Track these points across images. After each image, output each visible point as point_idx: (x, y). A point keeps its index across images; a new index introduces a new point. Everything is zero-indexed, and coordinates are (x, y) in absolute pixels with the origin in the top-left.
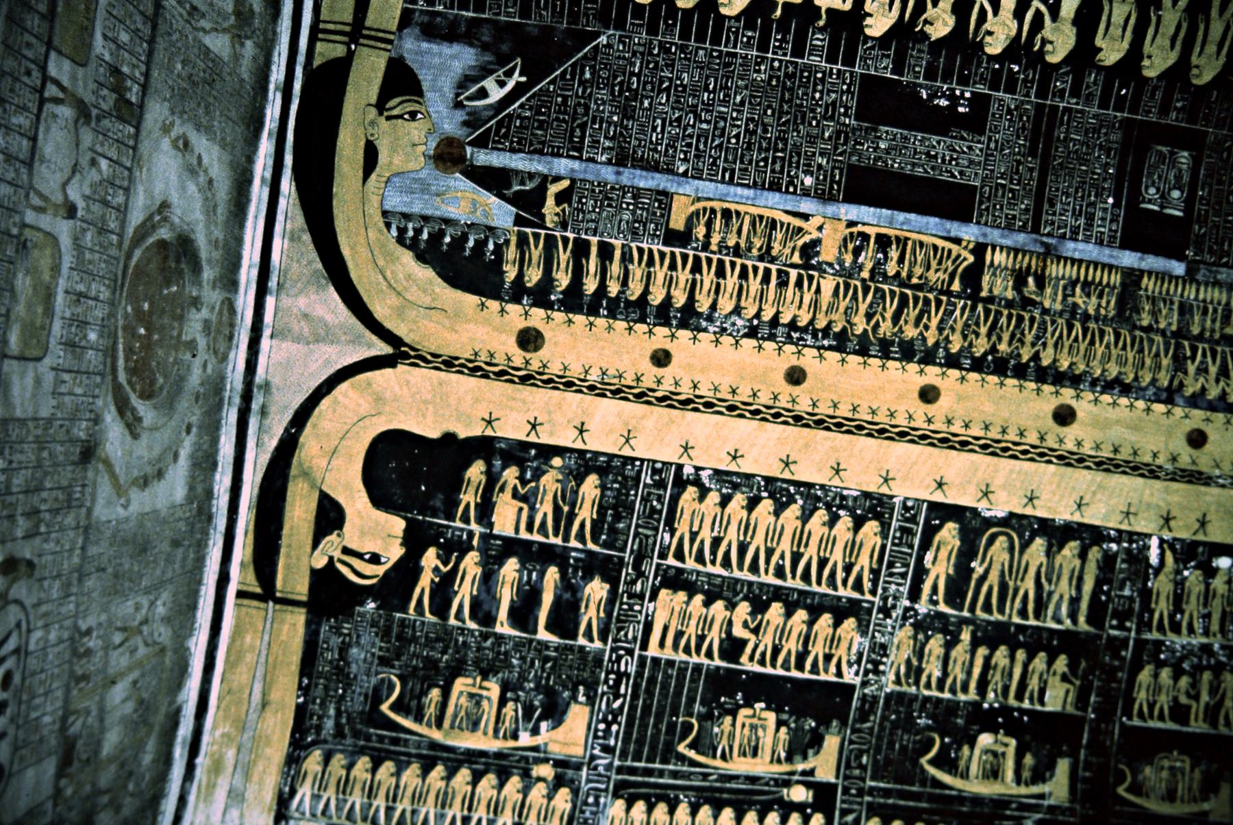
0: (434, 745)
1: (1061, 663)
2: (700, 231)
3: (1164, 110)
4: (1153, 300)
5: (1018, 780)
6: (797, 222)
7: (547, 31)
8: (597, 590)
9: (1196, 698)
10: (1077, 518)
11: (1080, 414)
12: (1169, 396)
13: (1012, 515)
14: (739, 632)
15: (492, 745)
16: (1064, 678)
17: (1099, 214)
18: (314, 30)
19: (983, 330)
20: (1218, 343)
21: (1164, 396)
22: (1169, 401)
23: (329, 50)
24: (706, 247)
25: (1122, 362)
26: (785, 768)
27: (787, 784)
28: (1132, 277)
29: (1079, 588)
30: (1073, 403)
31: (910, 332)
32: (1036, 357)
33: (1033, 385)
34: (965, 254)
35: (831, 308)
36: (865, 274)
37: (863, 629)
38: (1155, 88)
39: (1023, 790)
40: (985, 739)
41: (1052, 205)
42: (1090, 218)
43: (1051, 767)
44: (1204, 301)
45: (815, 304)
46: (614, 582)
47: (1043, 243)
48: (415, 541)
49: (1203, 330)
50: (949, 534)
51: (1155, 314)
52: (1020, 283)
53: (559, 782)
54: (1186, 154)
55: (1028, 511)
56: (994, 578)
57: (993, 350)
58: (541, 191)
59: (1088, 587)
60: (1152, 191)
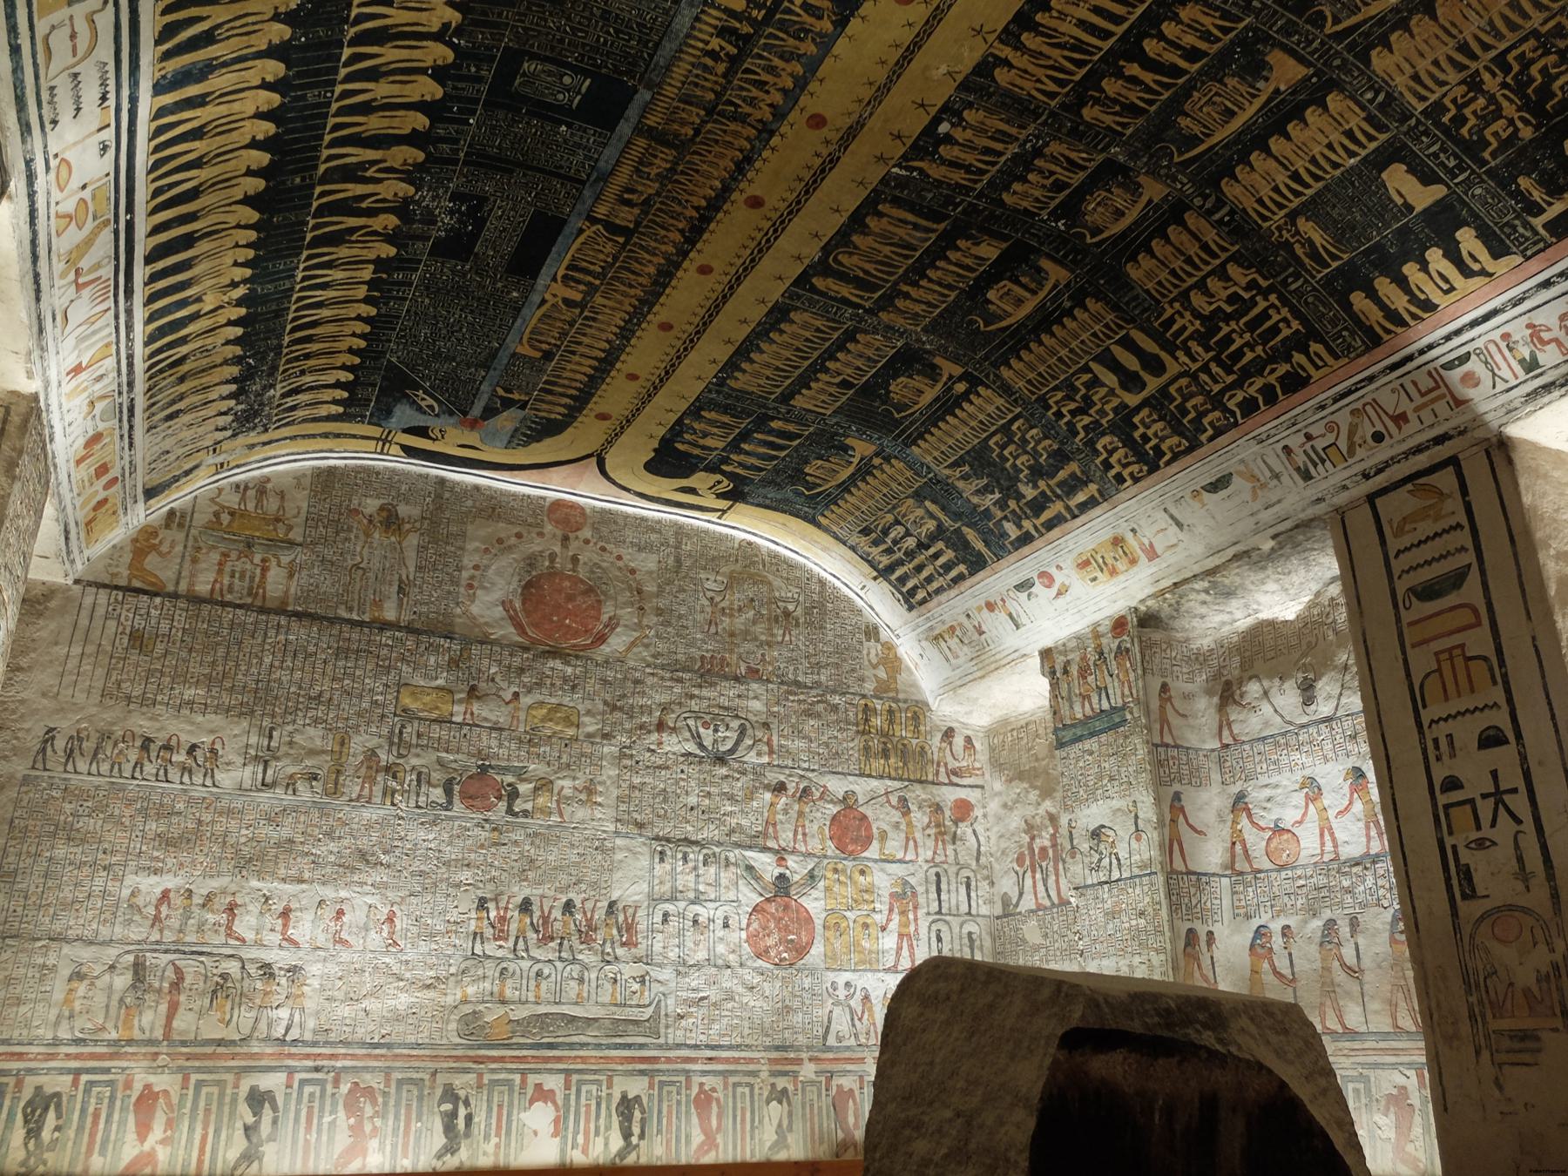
0: (839, 486)
1: (961, 243)
2: (545, 346)
3: (479, 79)
4: (669, 121)
5: (1034, 292)
6: (547, 306)
7: (384, 378)
8: (775, 424)
9: (1052, 173)
10: (846, 215)
11: (758, 193)
12: (766, 131)
13: (823, 248)
14: (837, 380)
15: (851, 470)
16: (978, 244)
17: (577, 139)
18: (382, 453)
19: (663, 233)
20: (730, 82)
21: (765, 135)
22: (772, 133)
23: (395, 449)
24: (559, 347)
25: (722, 156)
26: (940, 385)
27: (950, 389)
28: (639, 130)
29: (906, 222)
30: (745, 196)
31: (652, 270)
32: (697, 209)
33: (720, 215)
34: (594, 228)
35: (621, 303)
36: (597, 282)
37: (866, 332)
38: (455, 88)
39: (1042, 295)
40: (991, 295)
41: (561, 167)
42: (579, 146)
43: (1039, 270)
44: (683, 83)
45: (613, 309)
46: (773, 419)
47: (595, 181)
48: (712, 469)
49: (712, 90)
50: (818, 282)
51: (683, 123)
52: (628, 203)
53: (887, 459)
54: (526, 65)
55: (825, 240)
56: (867, 266)
57: (682, 231)
58: (501, 398)
59: (910, 217)
60: (560, 97)
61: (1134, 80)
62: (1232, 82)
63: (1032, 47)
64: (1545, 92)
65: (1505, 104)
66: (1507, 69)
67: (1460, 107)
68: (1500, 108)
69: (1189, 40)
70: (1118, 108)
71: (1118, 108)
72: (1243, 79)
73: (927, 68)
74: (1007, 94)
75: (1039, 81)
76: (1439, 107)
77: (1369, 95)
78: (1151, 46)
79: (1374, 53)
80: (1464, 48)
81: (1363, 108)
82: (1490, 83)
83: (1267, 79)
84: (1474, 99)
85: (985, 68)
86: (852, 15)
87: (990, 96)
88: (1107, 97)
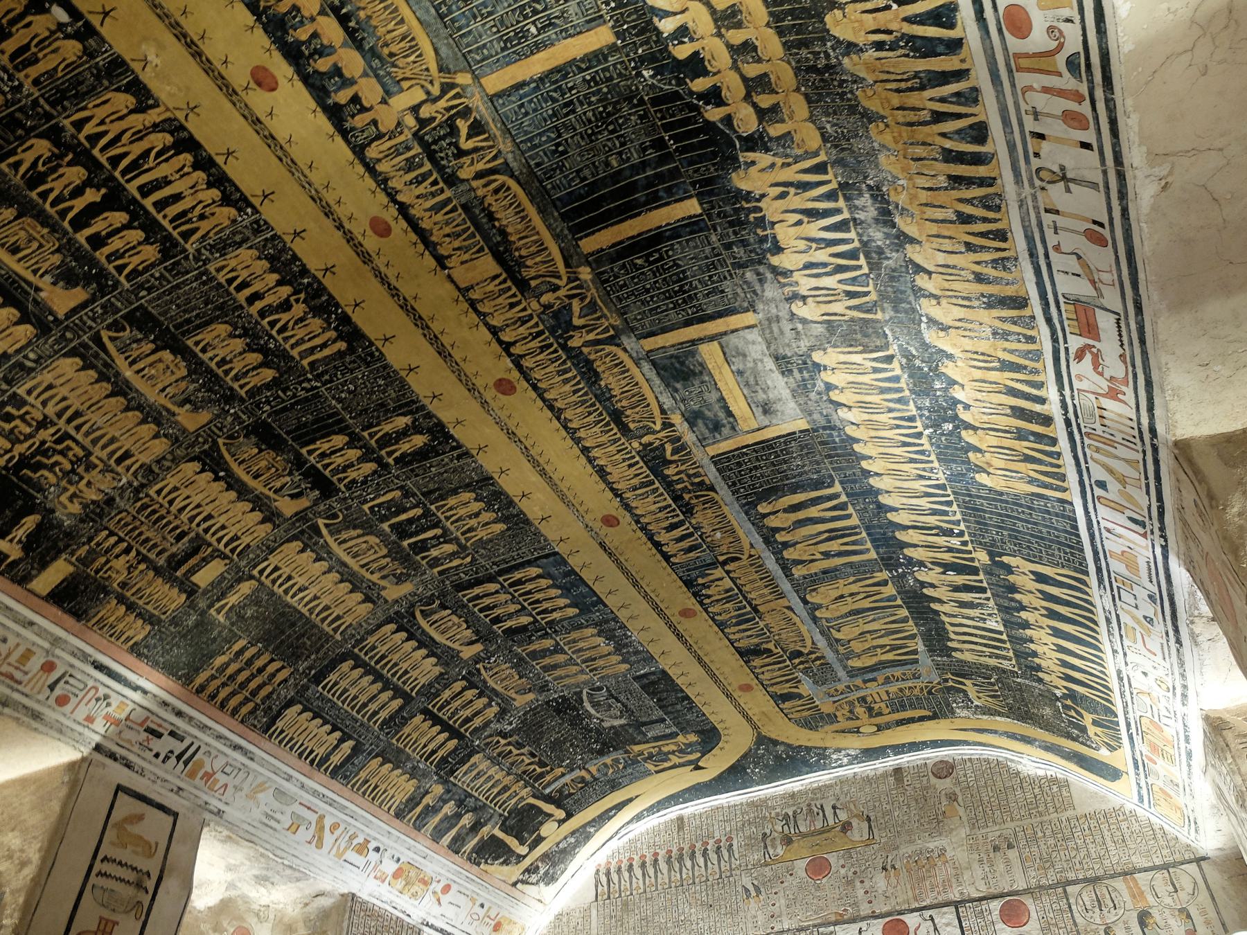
61: (78, 192)
62: (56, 259)
63: (152, 137)
64: (38, 467)
65: (26, 445)
66: (58, 441)
67: (22, 418)
68: (21, 442)
69: (116, 244)
70: (41, 168)
71: (41, 168)
72: (58, 267)
73: (161, 46)
74: (92, 91)
75: (102, 123)
76: (18, 402)
77: (32, 356)
78: (120, 218)
79: (77, 360)
80: (77, 414)
81: (18, 351)
82: (45, 434)
83: (54, 284)
84: (30, 425)
85: (143, 98)
86: (259, 19)
87: (98, 77)
88: (61, 166)
